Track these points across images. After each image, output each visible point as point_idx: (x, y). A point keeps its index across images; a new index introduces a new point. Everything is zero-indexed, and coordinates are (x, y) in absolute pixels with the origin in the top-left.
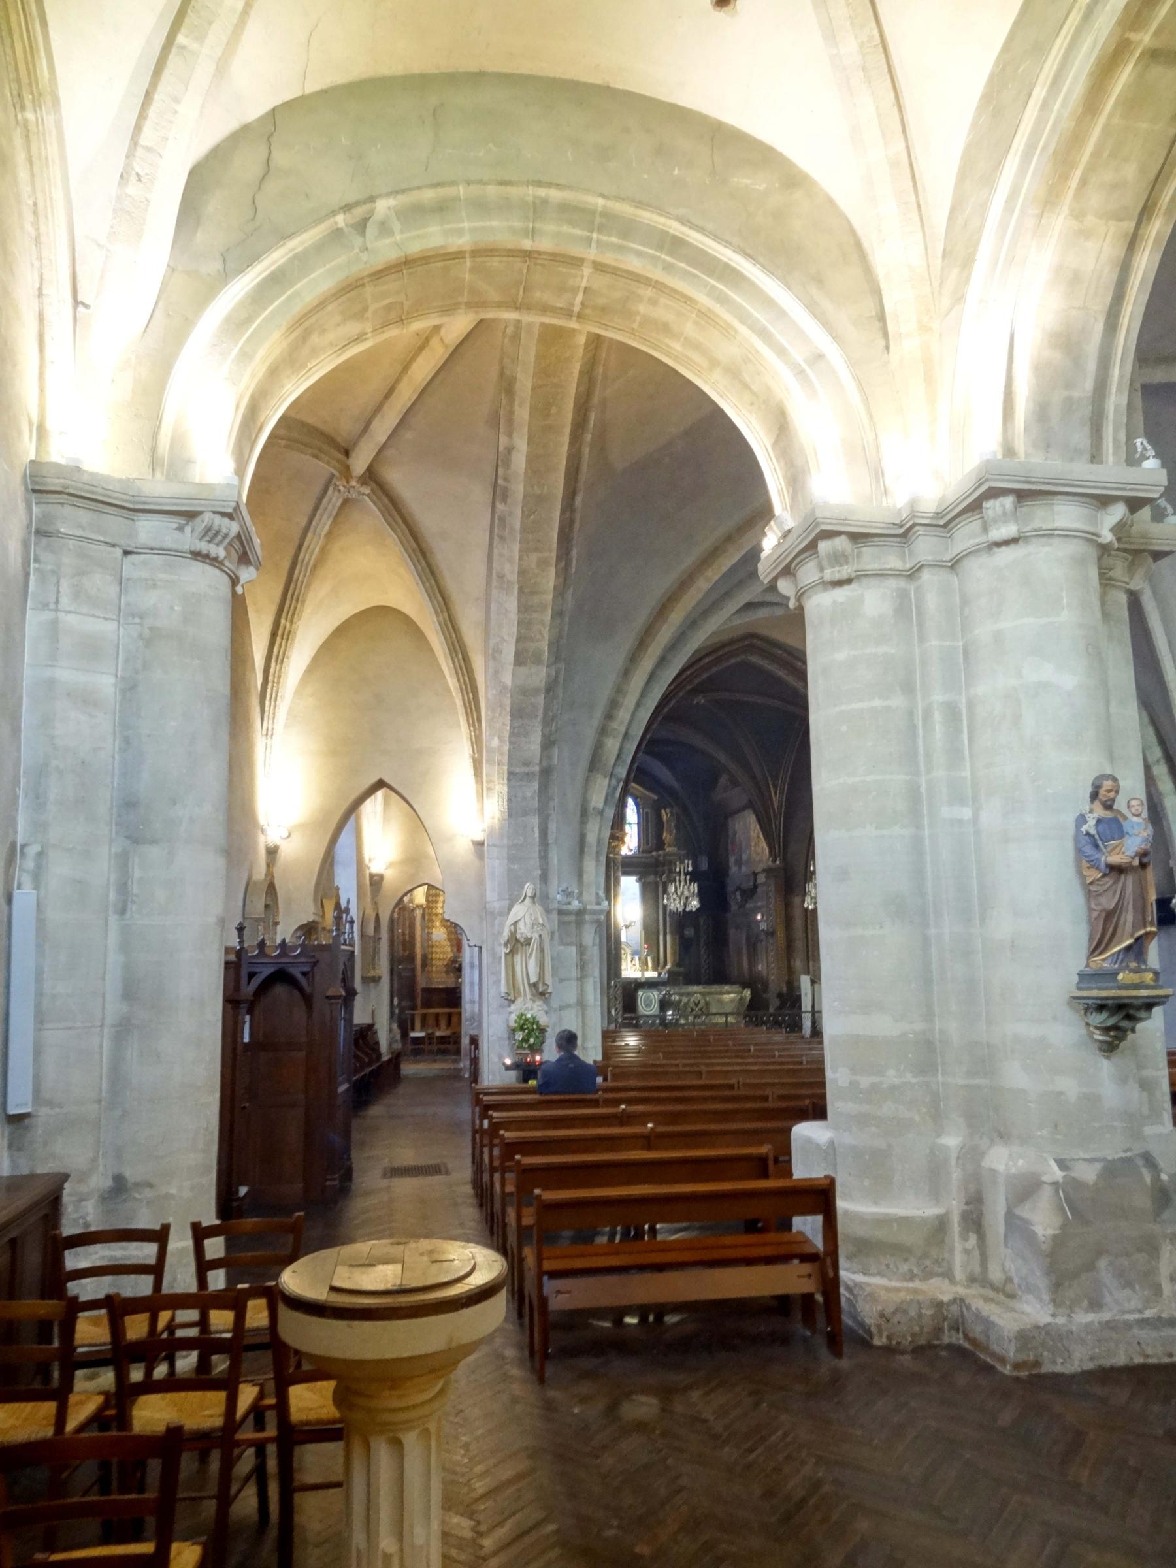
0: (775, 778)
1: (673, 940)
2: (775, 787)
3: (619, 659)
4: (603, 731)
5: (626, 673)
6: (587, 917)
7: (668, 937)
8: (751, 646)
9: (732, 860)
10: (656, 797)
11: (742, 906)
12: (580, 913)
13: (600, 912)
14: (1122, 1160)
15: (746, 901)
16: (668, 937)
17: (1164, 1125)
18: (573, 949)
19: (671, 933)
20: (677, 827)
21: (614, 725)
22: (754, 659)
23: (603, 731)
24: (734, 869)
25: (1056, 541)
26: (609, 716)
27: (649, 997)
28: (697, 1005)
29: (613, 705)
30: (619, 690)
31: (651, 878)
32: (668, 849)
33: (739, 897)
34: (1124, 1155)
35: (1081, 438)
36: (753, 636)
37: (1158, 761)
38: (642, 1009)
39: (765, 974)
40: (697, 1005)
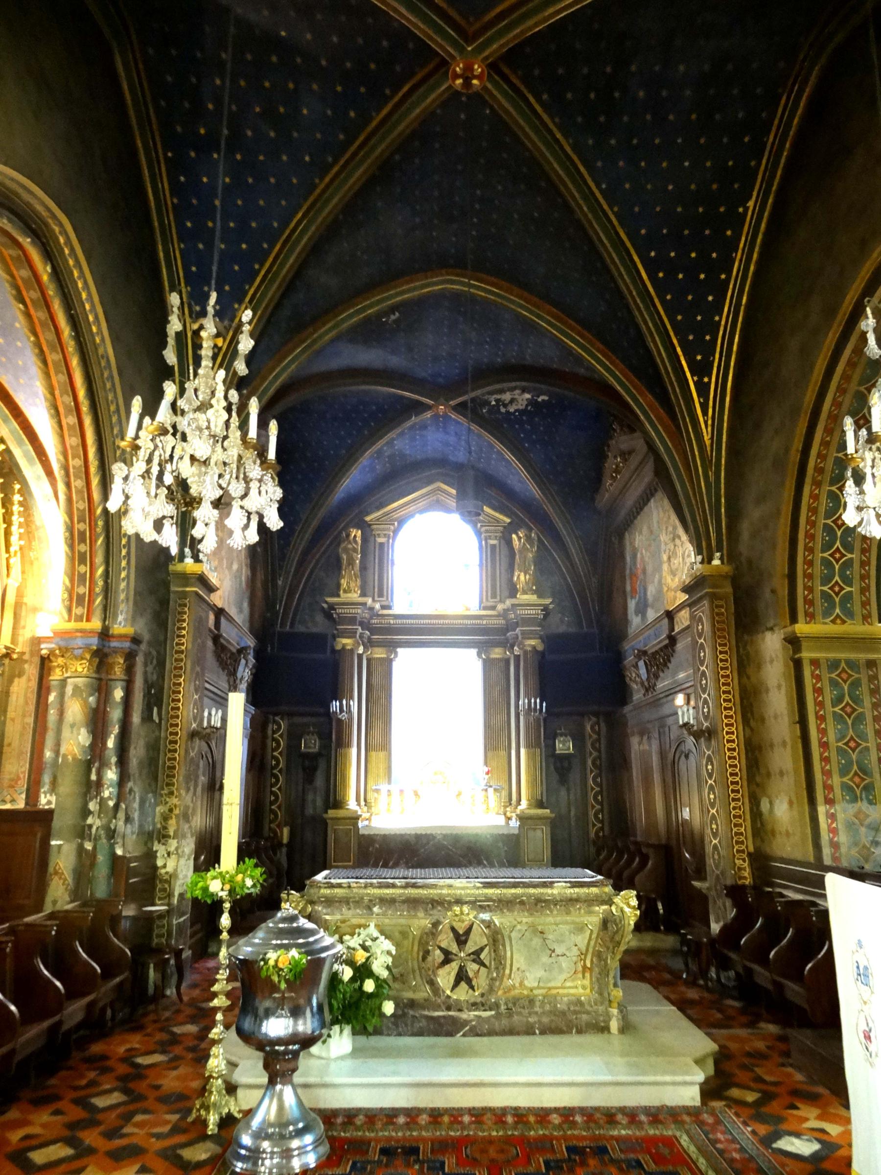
0: (701, 370)
1: (531, 757)
7: (523, 751)
9: (632, 605)
10: (508, 520)
11: (649, 688)
15: (657, 677)
16: (523, 751)
19: (528, 746)
20: (539, 561)
24: (635, 621)
28: (461, 939)
31: (497, 653)
32: (523, 598)
33: (643, 671)
39: (697, 823)
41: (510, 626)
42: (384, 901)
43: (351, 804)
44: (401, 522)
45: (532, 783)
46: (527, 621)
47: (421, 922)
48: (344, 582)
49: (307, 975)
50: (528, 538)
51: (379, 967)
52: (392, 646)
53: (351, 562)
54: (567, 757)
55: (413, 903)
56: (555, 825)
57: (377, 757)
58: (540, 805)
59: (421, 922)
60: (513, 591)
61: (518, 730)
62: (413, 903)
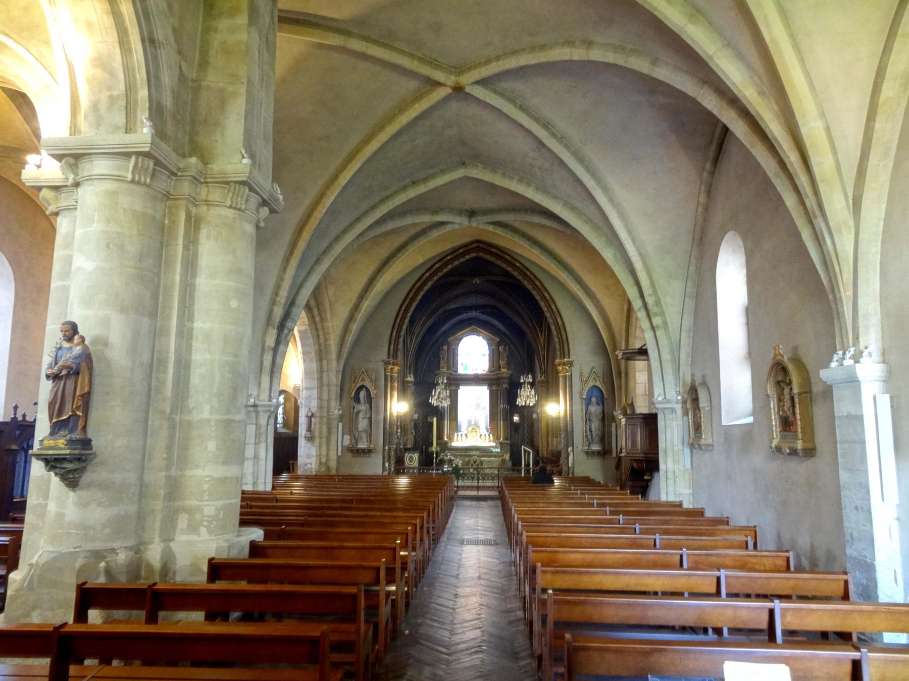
2: (541, 332)
3: (278, 261)
4: (273, 302)
5: (284, 268)
6: (260, 409)
8: (478, 247)
12: (255, 406)
13: (270, 406)
14: (70, 553)
17: (199, 535)
18: (254, 427)
21: (278, 299)
22: (481, 254)
23: (273, 302)
25: (95, 182)
26: (276, 294)
27: (411, 457)
29: (278, 287)
30: (281, 279)
31: (494, 388)
34: (73, 550)
35: (120, 119)
36: (478, 241)
37: (640, 309)
38: (407, 462)
40: (475, 462)
41: (498, 379)
42: (461, 456)
43: (446, 439)
44: (461, 339)
45: (504, 431)
46: (504, 378)
47: (467, 459)
48: (442, 365)
49: (450, 461)
50: (505, 349)
51: (460, 465)
52: (458, 386)
53: (444, 358)
54: (516, 424)
55: (466, 456)
56: (511, 445)
57: (453, 423)
58: (507, 439)
59: (467, 459)
60: (499, 368)
61: (500, 416)
62: (466, 456)
